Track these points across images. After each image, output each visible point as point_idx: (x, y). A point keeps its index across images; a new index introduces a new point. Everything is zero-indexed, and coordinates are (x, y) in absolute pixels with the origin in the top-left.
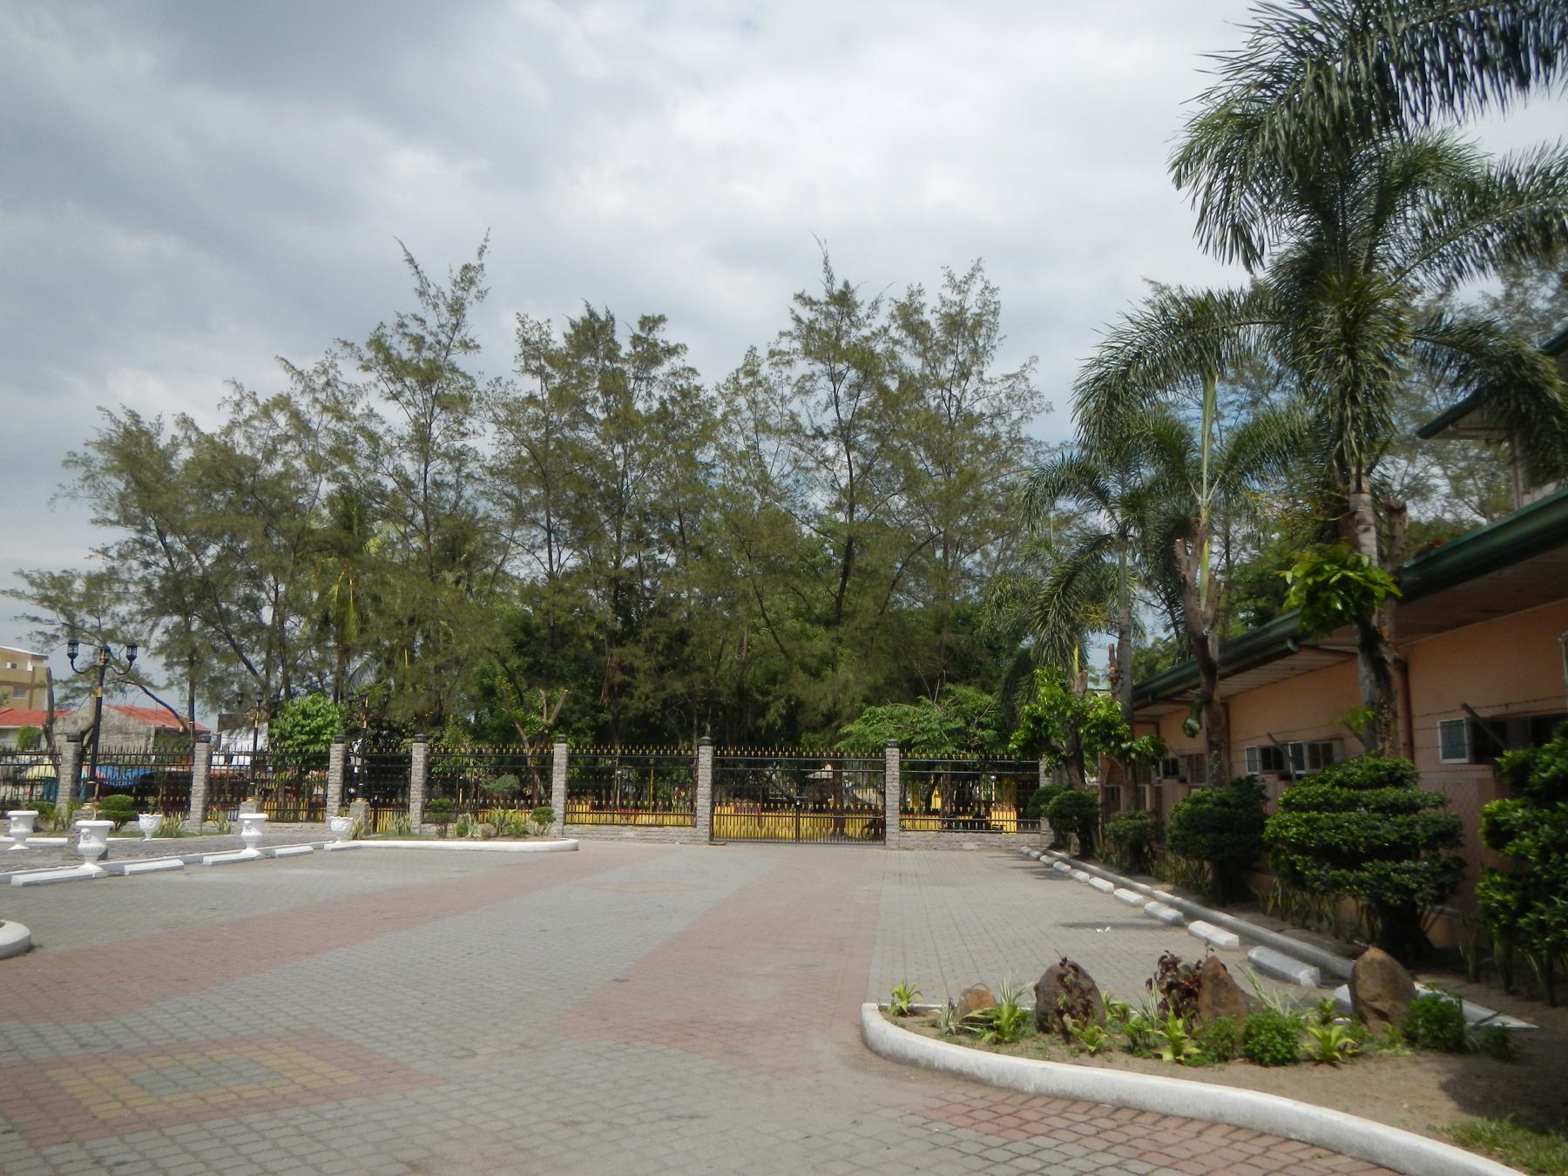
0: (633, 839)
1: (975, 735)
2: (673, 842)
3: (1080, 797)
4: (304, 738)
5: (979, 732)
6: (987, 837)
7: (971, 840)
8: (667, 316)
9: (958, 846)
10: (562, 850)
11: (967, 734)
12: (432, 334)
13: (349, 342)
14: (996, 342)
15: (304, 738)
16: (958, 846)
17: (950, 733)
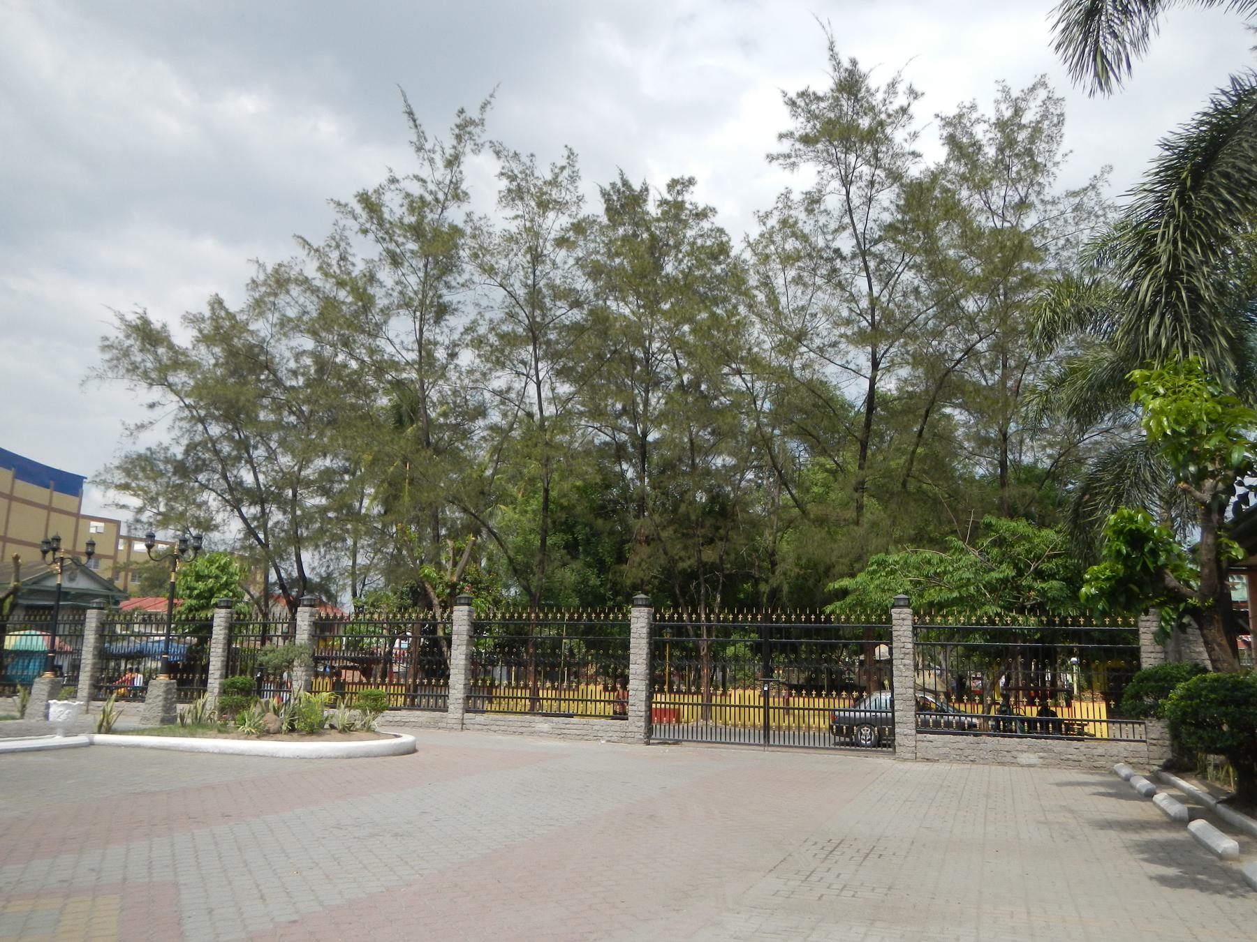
0: (549, 734)
1: (1031, 588)
2: (597, 738)
3: (1237, 686)
4: (194, 602)
5: (1038, 585)
6: (1058, 745)
7: (1029, 749)
8: (697, 178)
9: (1008, 758)
10: (368, 755)
11: (1018, 588)
12: (431, 193)
13: (343, 202)
14: (1058, 158)
15: (194, 602)
16: (1008, 758)
17: (991, 588)
